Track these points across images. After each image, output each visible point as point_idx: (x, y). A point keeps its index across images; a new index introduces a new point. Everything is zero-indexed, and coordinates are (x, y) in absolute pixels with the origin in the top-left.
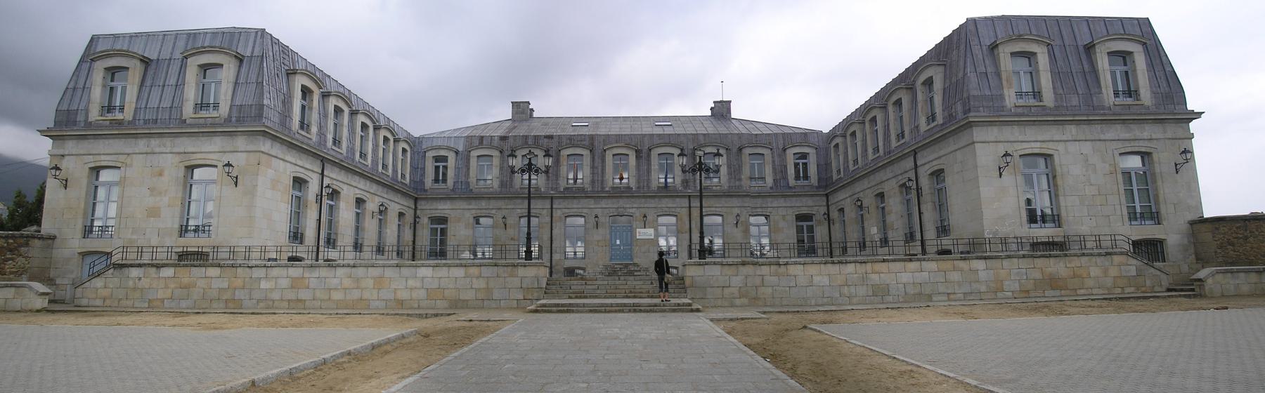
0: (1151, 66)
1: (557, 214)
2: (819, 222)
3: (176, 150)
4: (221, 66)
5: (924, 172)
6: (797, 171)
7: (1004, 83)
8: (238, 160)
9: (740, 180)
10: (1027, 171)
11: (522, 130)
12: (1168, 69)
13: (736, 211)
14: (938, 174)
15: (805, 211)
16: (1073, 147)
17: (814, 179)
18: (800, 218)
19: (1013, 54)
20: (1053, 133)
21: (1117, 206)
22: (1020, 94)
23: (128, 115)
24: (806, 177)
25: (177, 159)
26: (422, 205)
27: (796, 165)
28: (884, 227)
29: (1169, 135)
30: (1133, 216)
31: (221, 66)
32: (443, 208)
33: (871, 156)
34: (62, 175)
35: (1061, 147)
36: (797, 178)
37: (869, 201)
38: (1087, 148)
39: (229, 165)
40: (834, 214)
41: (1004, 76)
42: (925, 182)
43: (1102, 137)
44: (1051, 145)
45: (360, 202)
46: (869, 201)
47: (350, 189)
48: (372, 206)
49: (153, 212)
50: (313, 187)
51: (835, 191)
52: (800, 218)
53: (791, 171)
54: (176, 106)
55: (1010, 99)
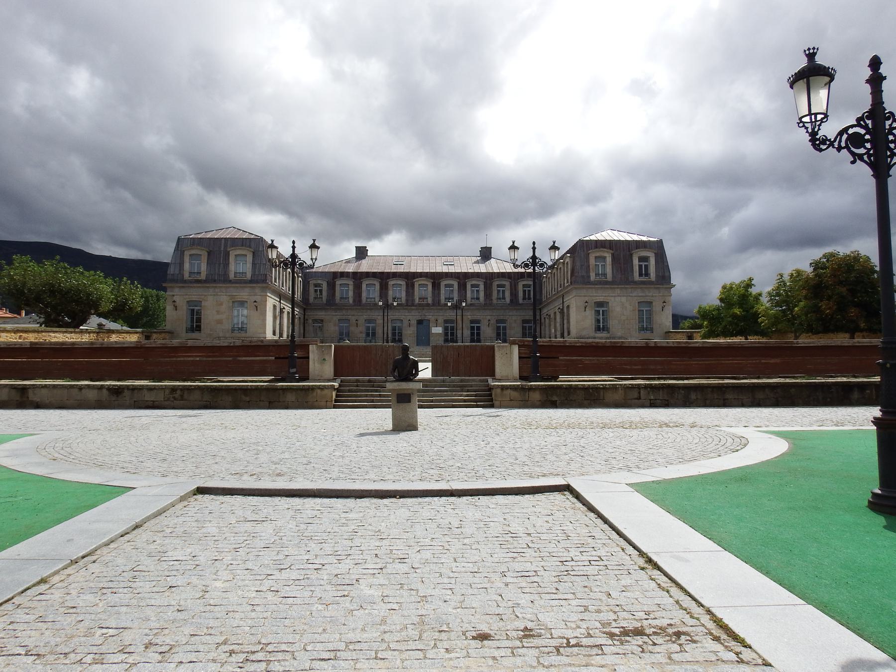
8: (258, 298)
11: (365, 266)
13: (489, 317)
14: (568, 307)
16: (618, 299)
19: (596, 257)
21: (636, 325)
22: (597, 275)
23: (203, 276)
27: (524, 291)
28: (555, 331)
30: (642, 329)
32: (321, 314)
35: (612, 299)
36: (524, 298)
38: (624, 299)
40: (543, 320)
46: (552, 316)
49: (220, 322)
50: (278, 310)
53: (521, 294)
54: (226, 274)
55: (593, 277)
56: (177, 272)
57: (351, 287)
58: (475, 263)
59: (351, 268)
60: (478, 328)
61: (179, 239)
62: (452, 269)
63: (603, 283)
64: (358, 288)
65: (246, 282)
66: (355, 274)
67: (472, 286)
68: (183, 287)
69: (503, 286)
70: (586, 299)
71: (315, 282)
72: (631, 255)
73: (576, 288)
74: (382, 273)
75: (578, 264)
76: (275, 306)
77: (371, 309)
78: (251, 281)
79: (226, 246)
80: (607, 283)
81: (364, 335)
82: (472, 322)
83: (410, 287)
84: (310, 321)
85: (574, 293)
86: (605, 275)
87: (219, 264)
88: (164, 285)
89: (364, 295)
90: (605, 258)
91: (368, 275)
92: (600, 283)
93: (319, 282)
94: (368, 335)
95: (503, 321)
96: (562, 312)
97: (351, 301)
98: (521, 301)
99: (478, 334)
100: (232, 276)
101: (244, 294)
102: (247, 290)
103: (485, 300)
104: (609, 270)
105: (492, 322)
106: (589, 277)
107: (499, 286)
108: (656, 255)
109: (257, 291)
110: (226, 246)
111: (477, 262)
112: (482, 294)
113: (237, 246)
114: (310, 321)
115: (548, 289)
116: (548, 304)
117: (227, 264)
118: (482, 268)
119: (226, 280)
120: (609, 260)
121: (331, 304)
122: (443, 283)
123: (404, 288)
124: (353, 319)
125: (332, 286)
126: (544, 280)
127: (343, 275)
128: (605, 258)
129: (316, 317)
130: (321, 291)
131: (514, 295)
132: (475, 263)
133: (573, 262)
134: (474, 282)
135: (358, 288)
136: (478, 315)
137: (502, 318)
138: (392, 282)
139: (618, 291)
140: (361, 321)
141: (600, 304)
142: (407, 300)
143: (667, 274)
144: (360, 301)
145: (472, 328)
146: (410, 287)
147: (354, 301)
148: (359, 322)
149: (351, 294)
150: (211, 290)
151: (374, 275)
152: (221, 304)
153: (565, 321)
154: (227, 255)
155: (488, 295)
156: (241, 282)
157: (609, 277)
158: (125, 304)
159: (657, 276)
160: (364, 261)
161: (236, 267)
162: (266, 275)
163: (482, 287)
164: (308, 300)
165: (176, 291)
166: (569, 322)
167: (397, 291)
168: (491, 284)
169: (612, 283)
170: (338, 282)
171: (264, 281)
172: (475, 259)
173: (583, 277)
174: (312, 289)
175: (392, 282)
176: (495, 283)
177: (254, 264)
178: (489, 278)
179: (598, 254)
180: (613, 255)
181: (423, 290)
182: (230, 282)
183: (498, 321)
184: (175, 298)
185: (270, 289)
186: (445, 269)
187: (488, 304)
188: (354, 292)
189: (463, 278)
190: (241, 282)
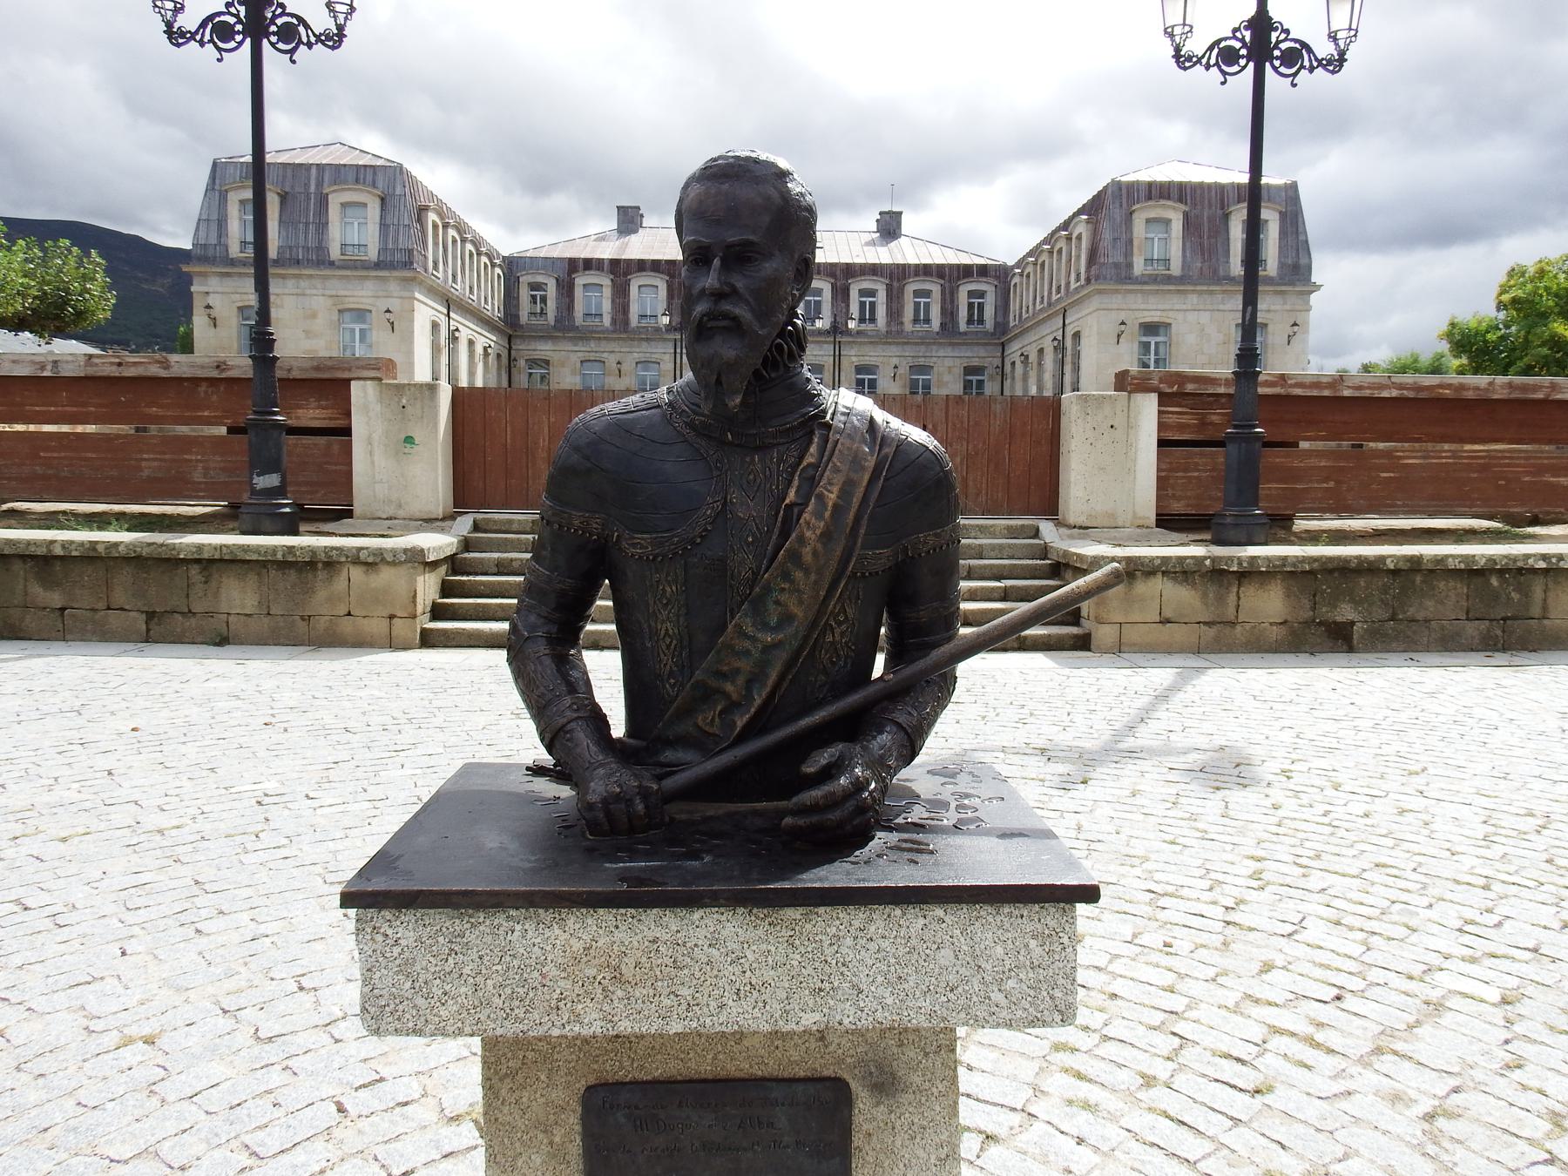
0: (1283, 233)
2: (991, 378)
3: (328, 292)
4: (365, 205)
5: (1070, 331)
6: (970, 315)
7: (1135, 250)
8: (394, 304)
10: (1145, 339)
12: (1302, 238)
13: (895, 361)
14: (1077, 336)
15: (975, 362)
16: (1192, 316)
17: (989, 324)
18: (969, 370)
19: (1148, 221)
20: (1175, 302)
22: (1149, 261)
24: (981, 321)
25: (330, 302)
26: (519, 345)
27: (971, 306)
29: (1288, 307)
31: (365, 205)
32: (544, 349)
33: (1038, 307)
34: (214, 313)
35: (1180, 316)
36: (970, 321)
37: (1033, 357)
38: (1205, 317)
39: (388, 311)
40: (1008, 368)
41: (1136, 243)
42: (1069, 343)
43: (1221, 307)
44: (1171, 314)
45: (471, 343)
46: (1033, 357)
47: (467, 330)
48: (479, 350)
50: (444, 333)
51: (1010, 340)
52: (969, 370)
54: (321, 248)
55: (1139, 267)
56: (213, 240)
57: (607, 292)
58: (867, 244)
59: (606, 252)
61: (215, 164)
63: (1161, 281)
64: (621, 293)
65: (365, 266)
66: (615, 263)
67: (863, 293)
68: (228, 275)
69: (927, 294)
70: (1122, 316)
71: (530, 279)
72: (1226, 217)
73: (1100, 292)
75: (1107, 236)
76: (435, 326)
77: (647, 340)
78: (378, 265)
79: (320, 184)
80: (1169, 279)
82: (860, 369)
84: (522, 363)
85: (1095, 302)
86: (1167, 261)
87: (307, 224)
88: (185, 269)
89: (634, 310)
90: (1167, 222)
91: (641, 266)
92: (1154, 279)
93: (540, 279)
95: (925, 369)
96: (1060, 348)
97: (607, 321)
98: (963, 327)
100: (335, 253)
101: (363, 293)
102: (369, 284)
103: (888, 324)
104: (1176, 251)
105: (901, 371)
106: (1130, 265)
107: (917, 293)
108: (1283, 215)
109: (393, 287)
110: (320, 184)
111: (872, 243)
113: (346, 182)
114: (522, 363)
115: (1023, 300)
116: (1021, 333)
117: (322, 225)
118: (884, 255)
119: (321, 260)
120: (1177, 226)
121: (565, 327)
124: (611, 360)
125: (566, 289)
126: (1016, 280)
127: (588, 264)
128: (1167, 222)
129: (537, 355)
130: (544, 300)
131: (949, 313)
132: (867, 244)
133: (1095, 234)
135: (621, 293)
137: (922, 361)
139: (1193, 299)
140: (628, 366)
141: (1150, 328)
143: (1303, 261)
144: (626, 322)
147: (614, 321)
148: (624, 367)
149: (607, 306)
150: (290, 283)
152: (314, 316)
153: (1068, 368)
154: (323, 202)
155: (894, 313)
156: (355, 266)
157: (1176, 268)
158: (66, 302)
159: (1282, 265)
161: (344, 234)
162: (410, 251)
163: (881, 297)
164: (518, 317)
165: (214, 284)
166: (1077, 369)
168: (901, 290)
169: (1181, 280)
170: (580, 280)
171: (408, 264)
172: (868, 237)
173: (1116, 265)
174: (524, 294)
176: (910, 288)
177: (384, 226)
178: (897, 275)
179: (1152, 214)
180: (1186, 216)
182: (332, 264)
183: (914, 369)
184: (211, 300)
185: (421, 283)
187: (895, 334)
190: (355, 266)
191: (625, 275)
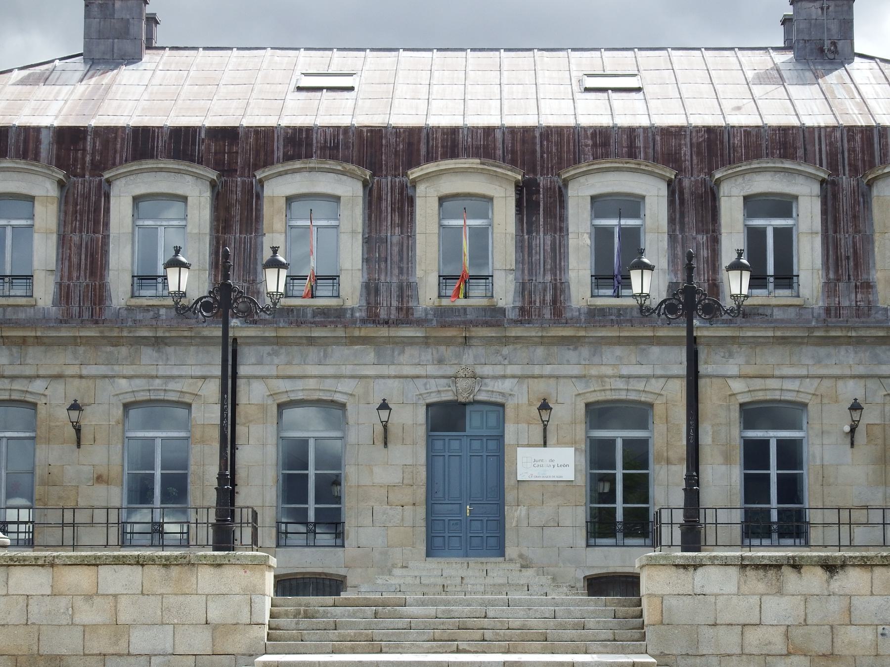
1: (253, 395)
9: (868, 286)
13: (851, 390)
57: (46, 216)
58: (763, 78)
59: (49, 108)
60: (791, 453)
62: (629, 113)
64: (84, 215)
66: (69, 139)
67: (755, 204)
74: (227, 135)
77: (158, 342)
81: (117, 495)
82: (753, 414)
83: (389, 210)
89: (121, 262)
91: (143, 143)
94: (141, 492)
97: (44, 292)
99: (791, 489)
103: (830, 288)
111: (777, 77)
112: (809, 256)
118: (808, 105)
122: (581, 191)
123: (353, 215)
124: (54, 401)
132: (763, 78)
134: (764, 184)
136: (785, 375)
138: (278, 187)
142: (371, 289)
144: (98, 294)
145: (754, 453)
146: (389, 210)
147: (64, 294)
148: (91, 419)
149: (44, 252)
151: (182, 144)
160: (126, 74)
163: (808, 216)
167: (316, 234)
175: (278, 187)
181: (465, 225)
186: (593, 113)
188: (63, 241)
189: (696, 159)
191: (98, 168)
